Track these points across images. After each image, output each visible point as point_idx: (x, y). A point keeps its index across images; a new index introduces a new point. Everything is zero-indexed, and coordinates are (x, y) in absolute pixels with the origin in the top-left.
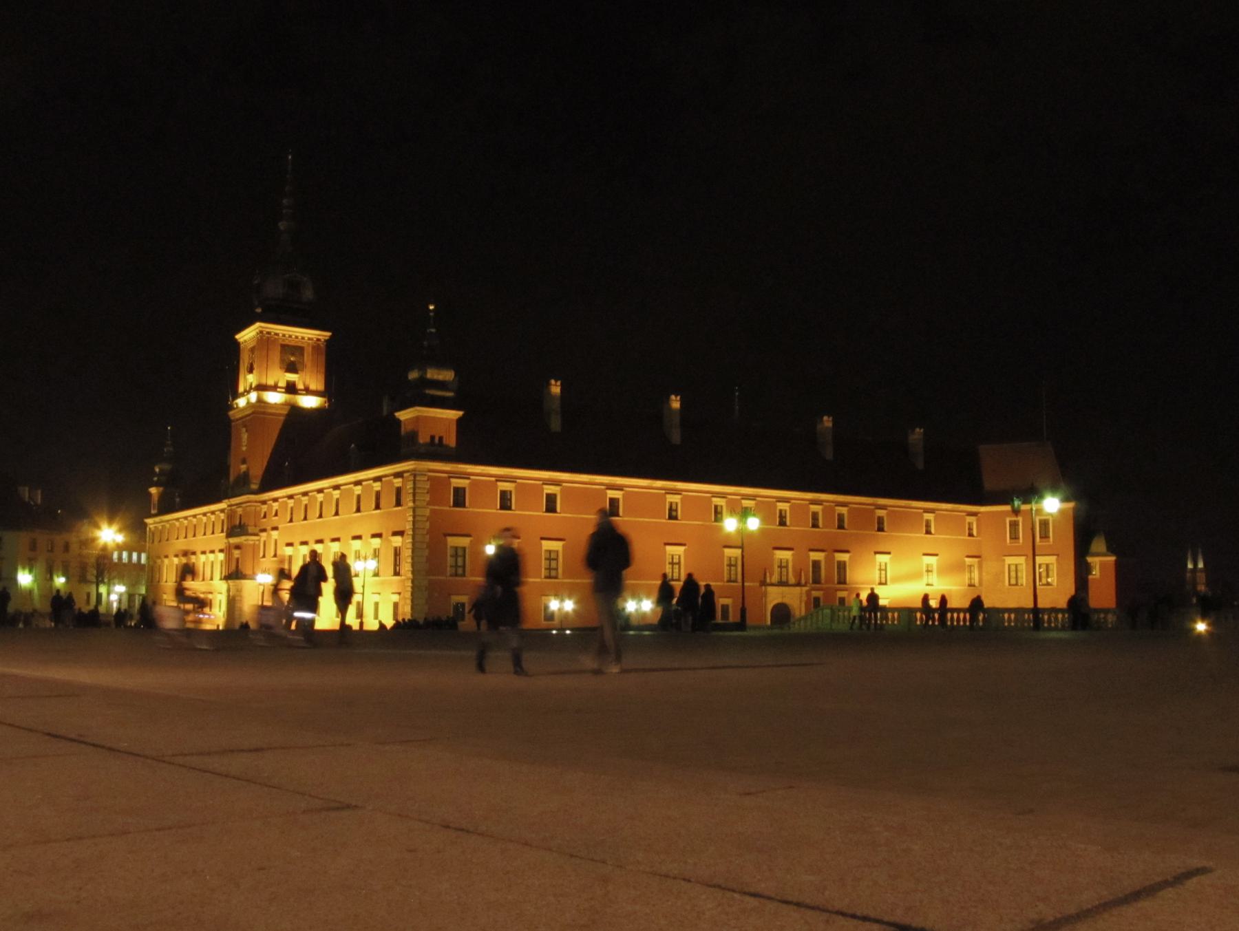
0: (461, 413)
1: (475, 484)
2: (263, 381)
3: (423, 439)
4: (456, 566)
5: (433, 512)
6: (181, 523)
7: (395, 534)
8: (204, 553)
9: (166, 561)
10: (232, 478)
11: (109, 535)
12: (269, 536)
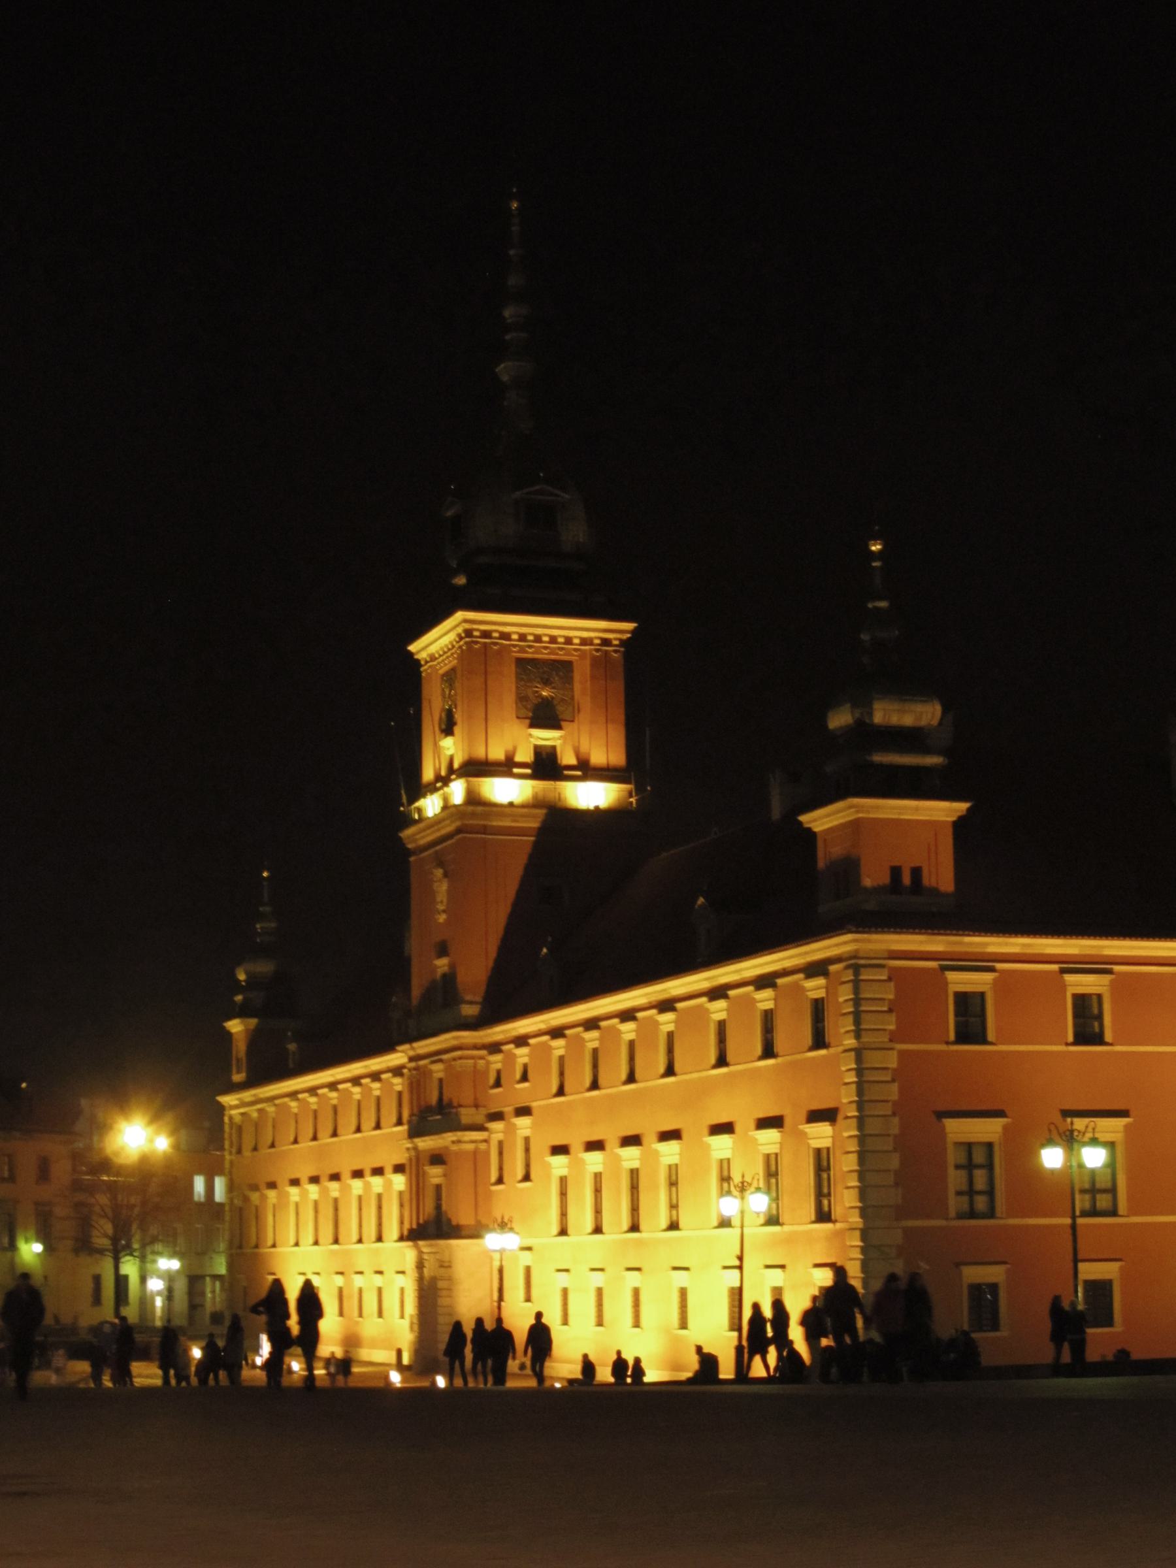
0: (962, 807)
1: (1005, 983)
2: (480, 753)
3: (873, 877)
4: (971, 1192)
5: (902, 1054)
6: (304, 1103)
7: (815, 1116)
8: (358, 1174)
9: (272, 1194)
10: (416, 992)
11: (138, 1137)
12: (511, 1130)
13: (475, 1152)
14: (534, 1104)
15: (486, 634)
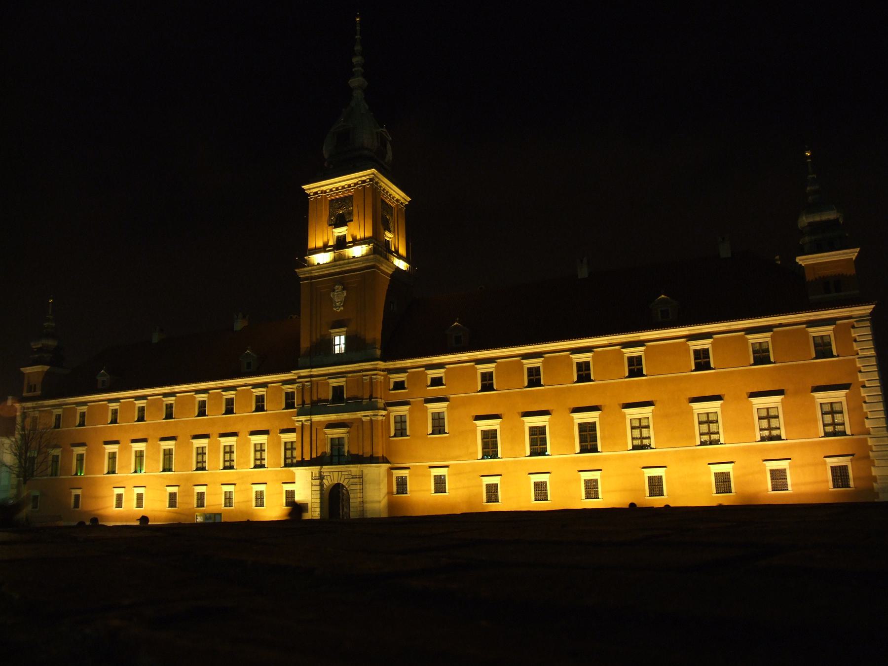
10: (305, 344)
13: (371, 421)
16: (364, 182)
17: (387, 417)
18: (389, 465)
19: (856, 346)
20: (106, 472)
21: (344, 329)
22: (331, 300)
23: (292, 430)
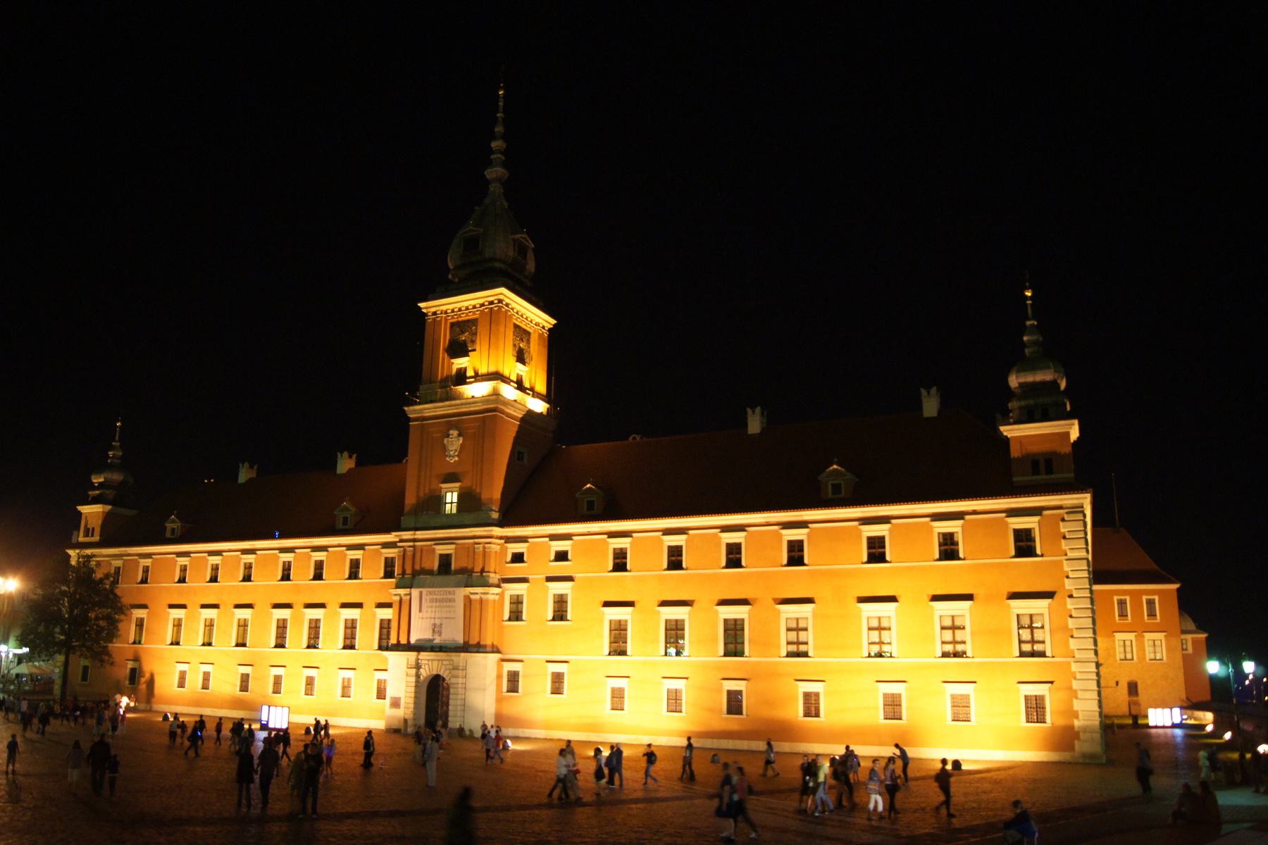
2: (501, 371)
10: (410, 500)
13: (481, 600)
14: (577, 576)
15: (507, 305)
16: (491, 303)
17: (502, 595)
18: (498, 656)
19: (1064, 545)
20: (169, 642)
21: (457, 485)
22: (444, 448)
23: (389, 605)
